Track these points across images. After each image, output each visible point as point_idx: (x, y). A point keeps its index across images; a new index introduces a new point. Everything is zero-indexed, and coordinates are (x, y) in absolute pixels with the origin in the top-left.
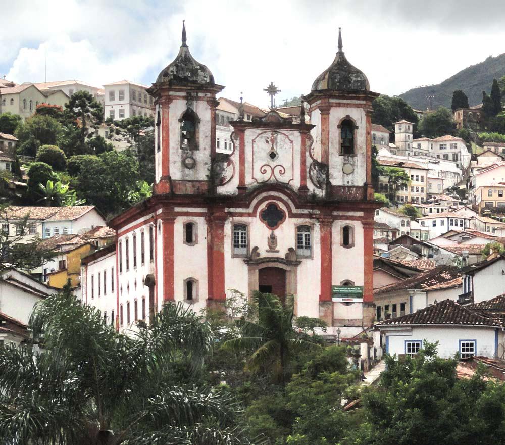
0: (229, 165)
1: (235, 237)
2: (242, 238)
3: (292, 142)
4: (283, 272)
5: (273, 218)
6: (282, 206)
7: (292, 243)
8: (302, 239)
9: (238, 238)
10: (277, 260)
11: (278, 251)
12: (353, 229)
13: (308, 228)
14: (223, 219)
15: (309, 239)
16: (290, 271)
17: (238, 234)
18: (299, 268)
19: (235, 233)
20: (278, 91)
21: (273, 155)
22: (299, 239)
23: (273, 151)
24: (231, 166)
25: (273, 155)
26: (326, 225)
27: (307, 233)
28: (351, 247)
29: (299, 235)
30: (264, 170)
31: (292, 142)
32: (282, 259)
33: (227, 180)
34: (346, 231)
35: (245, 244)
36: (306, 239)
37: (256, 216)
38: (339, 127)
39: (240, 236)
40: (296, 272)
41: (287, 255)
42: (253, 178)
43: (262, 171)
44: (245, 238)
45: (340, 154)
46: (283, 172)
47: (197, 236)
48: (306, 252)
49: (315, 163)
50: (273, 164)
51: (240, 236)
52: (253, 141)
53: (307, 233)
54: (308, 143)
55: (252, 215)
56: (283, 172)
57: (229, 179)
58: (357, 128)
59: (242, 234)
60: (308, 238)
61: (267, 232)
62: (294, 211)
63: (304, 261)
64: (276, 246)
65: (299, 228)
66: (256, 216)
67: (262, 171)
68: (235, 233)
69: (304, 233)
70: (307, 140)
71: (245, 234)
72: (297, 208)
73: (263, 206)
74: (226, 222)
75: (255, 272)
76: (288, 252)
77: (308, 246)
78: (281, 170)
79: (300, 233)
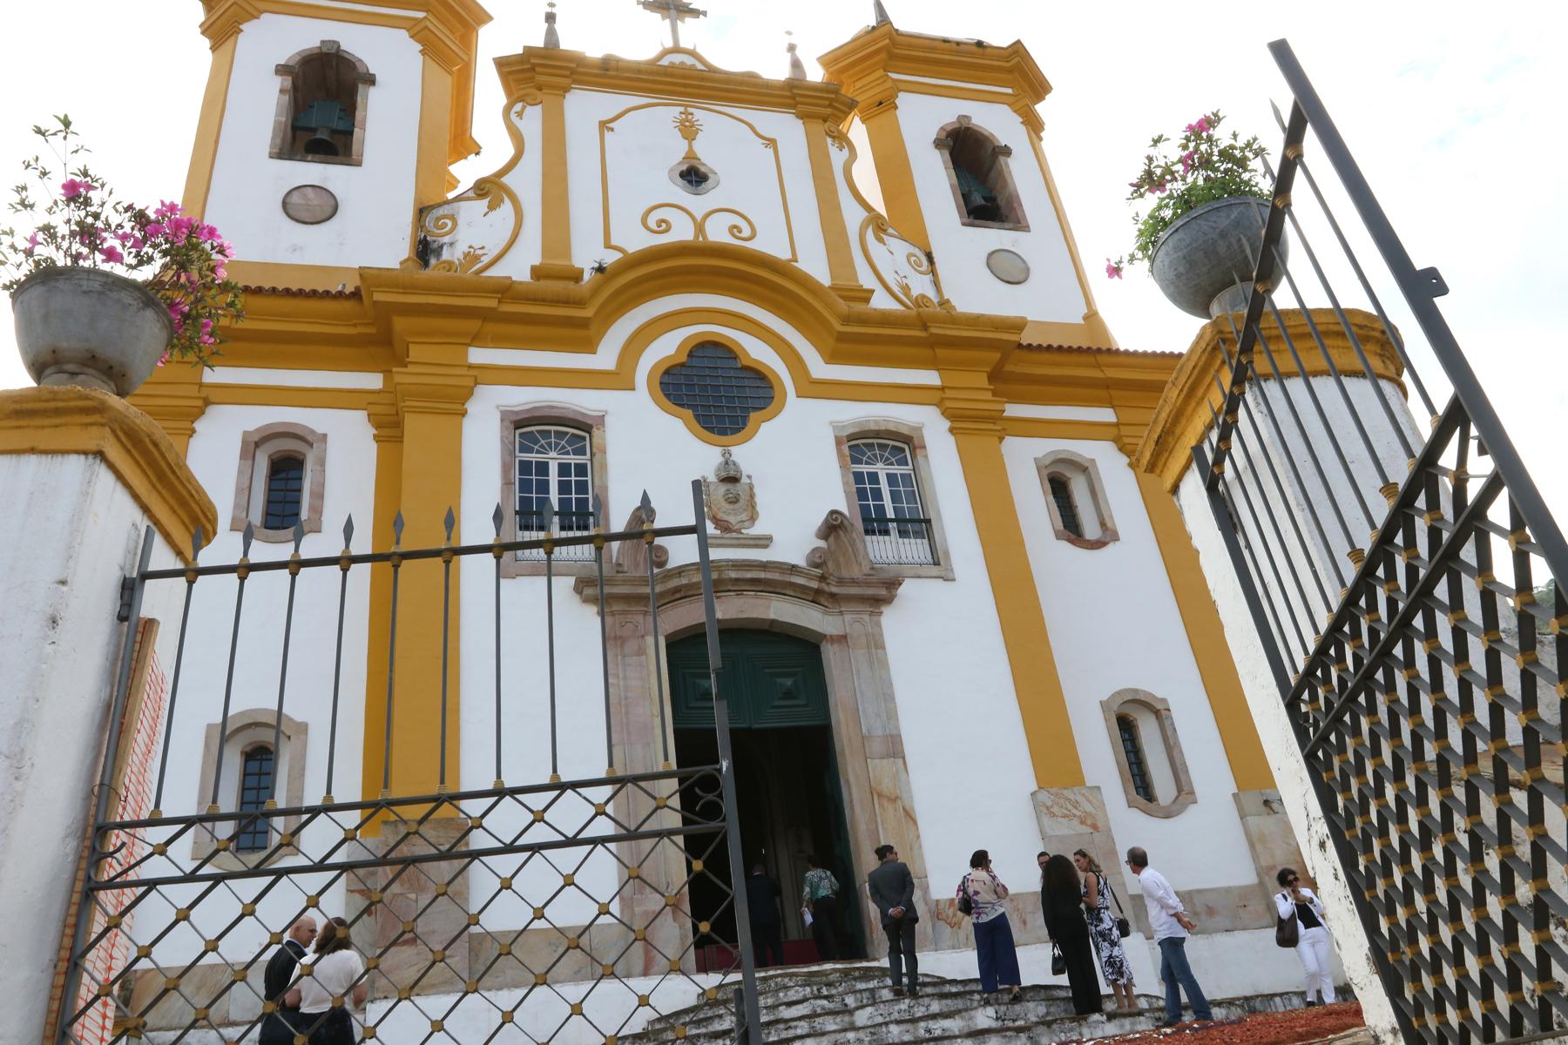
0: (491, 207)
1: (528, 478)
2: (564, 487)
3: (771, 143)
4: (803, 651)
5: (717, 393)
6: (757, 351)
7: (834, 495)
8: (877, 495)
9: (544, 487)
10: (774, 579)
11: (764, 542)
12: (1084, 468)
13: (901, 445)
14: (453, 403)
15: (911, 497)
16: (843, 639)
17: (543, 468)
18: (892, 621)
19: (525, 467)
20: (696, 13)
21: (694, 176)
22: (863, 488)
23: (695, 163)
24: (507, 206)
25: (694, 176)
26: (976, 426)
27: (898, 470)
28: (1098, 545)
29: (858, 477)
30: (663, 221)
31: (771, 143)
32: (793, 569)
33: (486, 260)
34: (1059, 488)
35: (581, 514)
36: (895, 497)
37: (631, 387)
38: (938, 144)
39: (554, 478)
40: (876, 643)
41: (818, 561)
42: (608, 246)
43: (652, 223)
44: (582, 488)
45: (966, 220)
46: (746, 232)
47: (319, 496)
48: (914, 549)
49: (878, 225)
50: (699, 204)
51: (554, 478)
52: (605, 126)
53: (898, 470)
54: (837, 157)
55: (619, 379)
56: (746, 232)
57: (496, 252)
58: (1007, 151)
59: (564, 469)
60: (911, 488)
61: (703, 458)
62: (820, 369)
63: (908, 589)
64: (753, 518)
65: (860, 446)
66: (631, 387)
67: (652, 223)
68: (525, 467)
69: (881, 470)
70: (829, 140)
71: (582, 470)
72: (832, 357)
73: (667, 347)
74: (473, 407)
75: (641, 652)
76: (822, 544)
77: (918, 524)
78: (735, 227)
79: (864, 469)
